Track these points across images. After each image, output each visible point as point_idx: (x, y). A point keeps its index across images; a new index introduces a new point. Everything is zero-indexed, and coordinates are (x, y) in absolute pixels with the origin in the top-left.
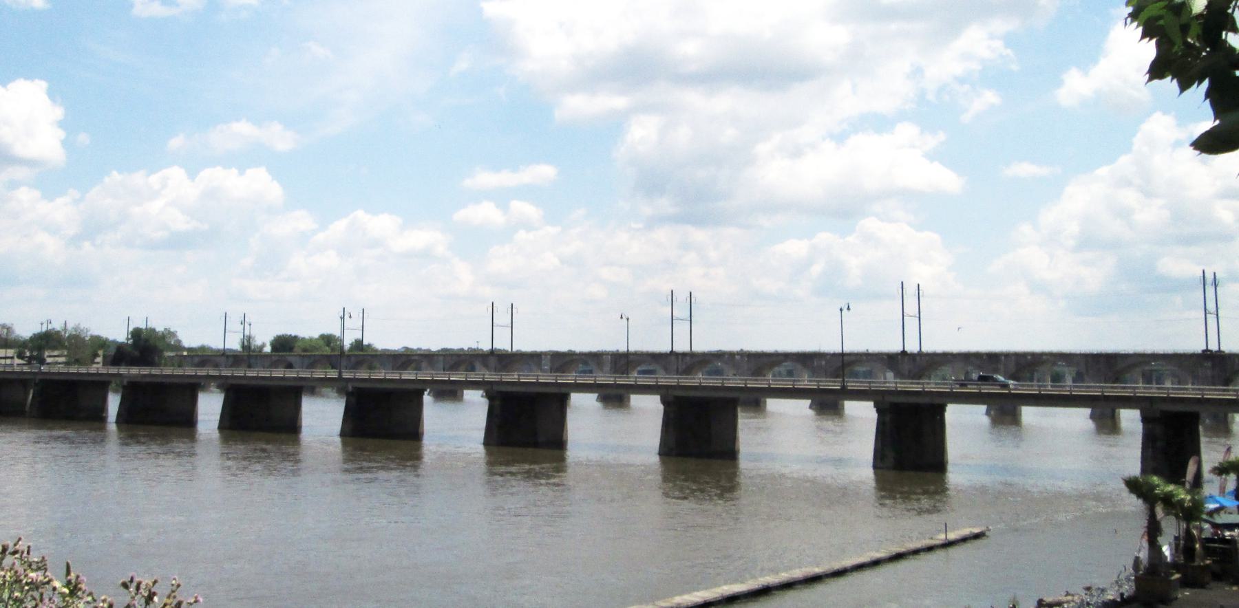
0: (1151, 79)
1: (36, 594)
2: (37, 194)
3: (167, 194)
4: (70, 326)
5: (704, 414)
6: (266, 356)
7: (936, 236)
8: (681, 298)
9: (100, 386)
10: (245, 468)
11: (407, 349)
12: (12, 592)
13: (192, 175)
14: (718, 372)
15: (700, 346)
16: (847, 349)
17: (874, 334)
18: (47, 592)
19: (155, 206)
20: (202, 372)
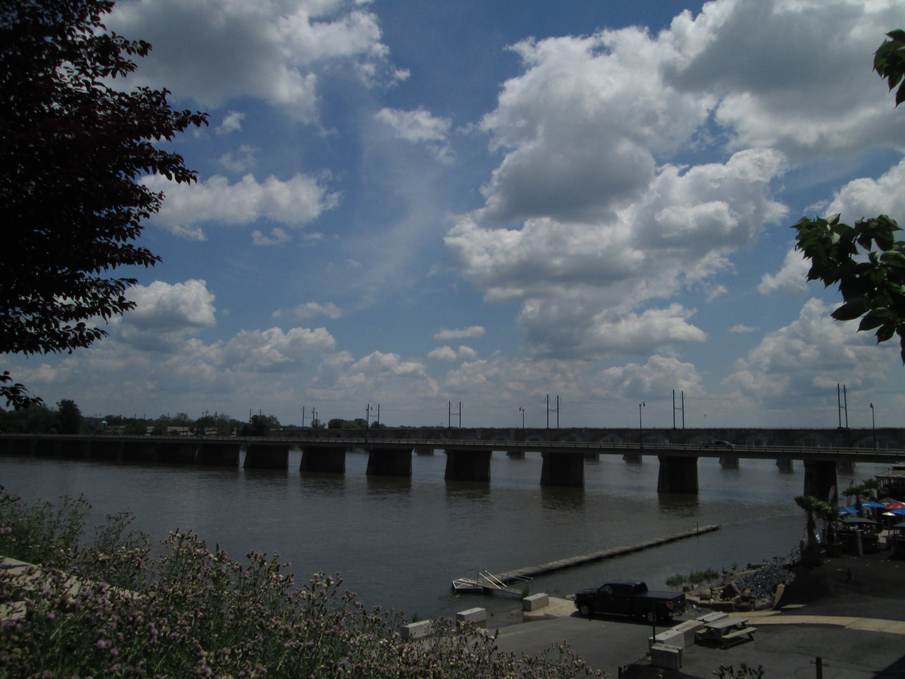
0: (809, 279)
1: (200, 561)
2: (200, 342)
3: (273, 342)
4: (219, 414)
5: (565, 459)
6: (326, 430)
7: (692, 365)
8: (553, 399)
9: (235, 447)
10: (314, 492)
11: (403, 427)
12: (187, 560)
13: (285, 331)
14: (573, 440)
15: (563, 425)
16: (644, 427)
17: (658, 418)
18: (206, 560)
19: (267, 348)
20: (291, 440)
